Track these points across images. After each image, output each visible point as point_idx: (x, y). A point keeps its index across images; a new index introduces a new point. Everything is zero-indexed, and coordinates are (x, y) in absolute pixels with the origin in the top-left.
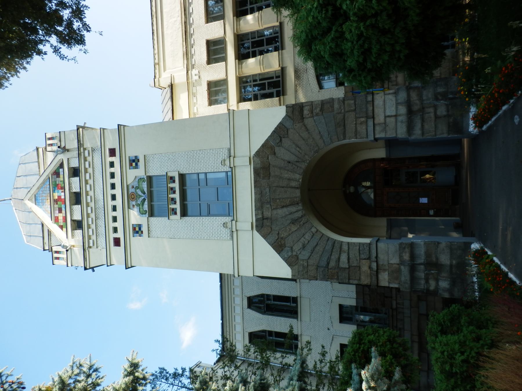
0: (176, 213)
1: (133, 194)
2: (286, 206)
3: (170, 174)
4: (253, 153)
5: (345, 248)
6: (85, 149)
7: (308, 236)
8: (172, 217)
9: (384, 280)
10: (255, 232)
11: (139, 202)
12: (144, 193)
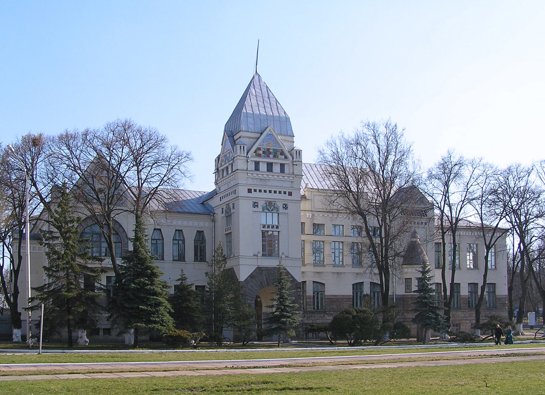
1: (272, 203)
3: (279, 227)
7: (256, 288)
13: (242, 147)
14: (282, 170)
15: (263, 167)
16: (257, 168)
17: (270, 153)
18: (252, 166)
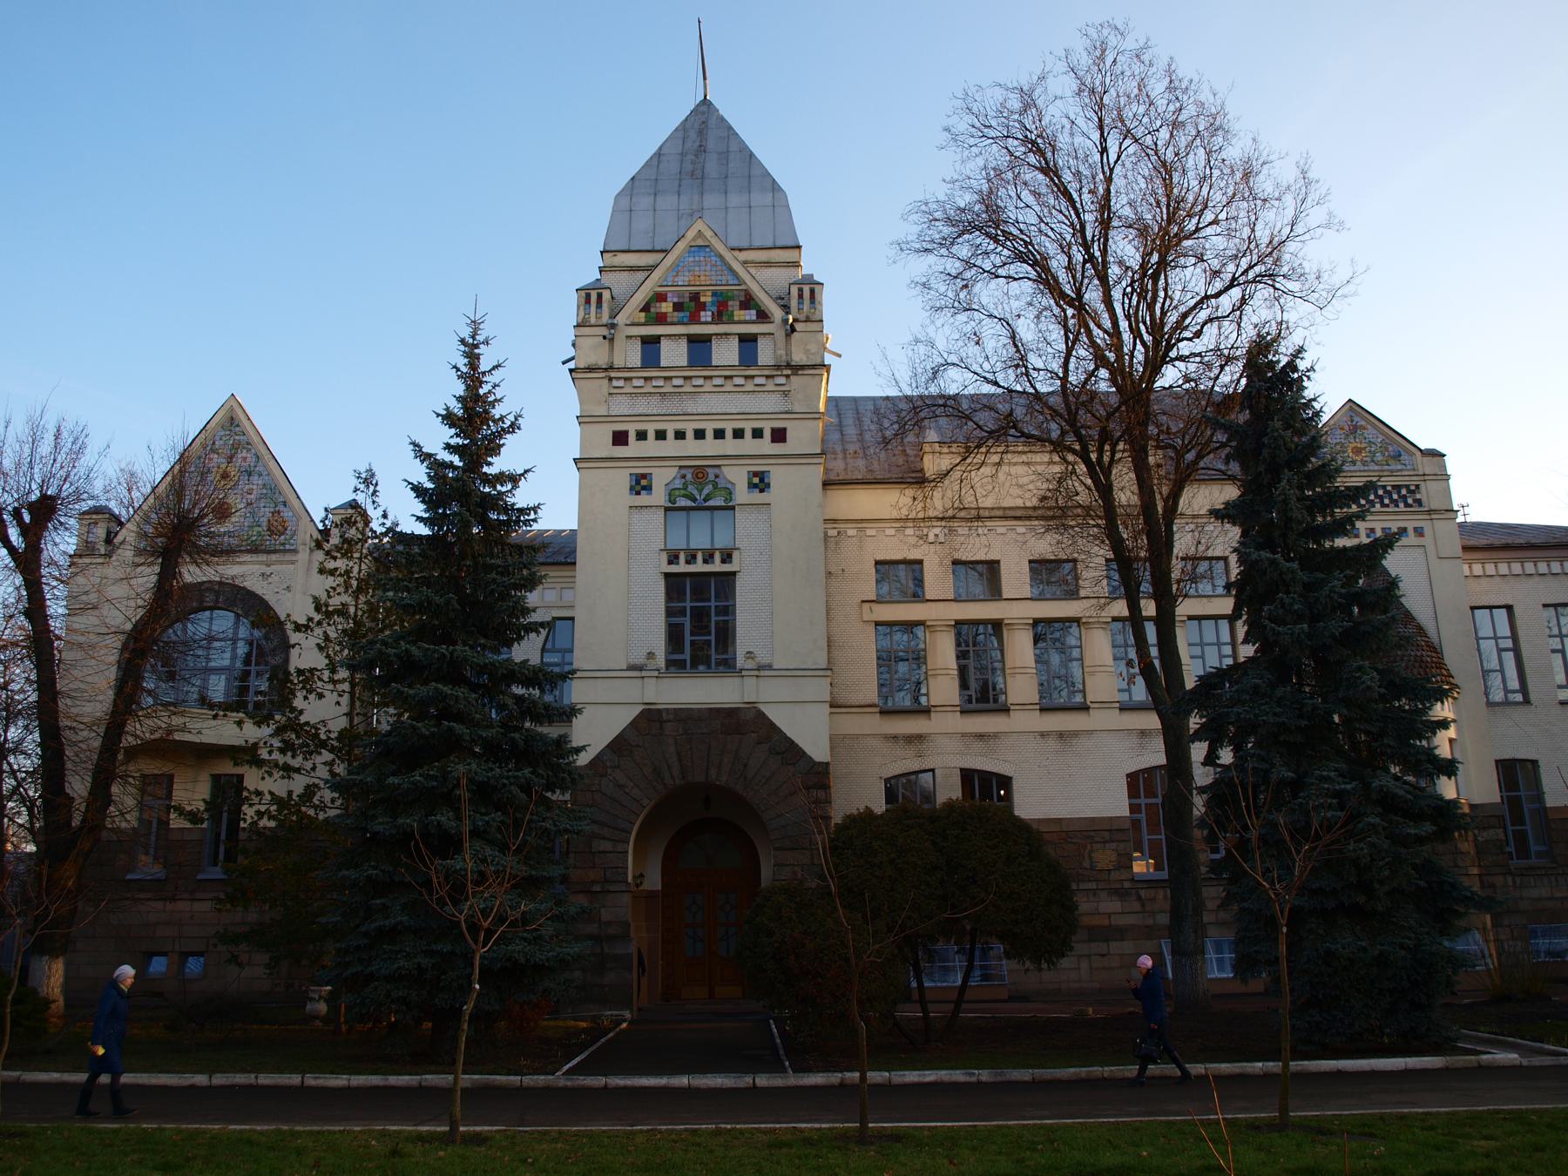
0: (670, 562)
1: (705, 475)
2: (680, 761)
3: (736, 555)
4: (763, 708)
5: (620, 848)
6: (788, 376)
8: (664, 557)
10: (641, 708)
11: (692, 489)
12: (705, 500)
13: (594, 298)
15: (674, 353)
17: (703, 306)
18: (634, 355)
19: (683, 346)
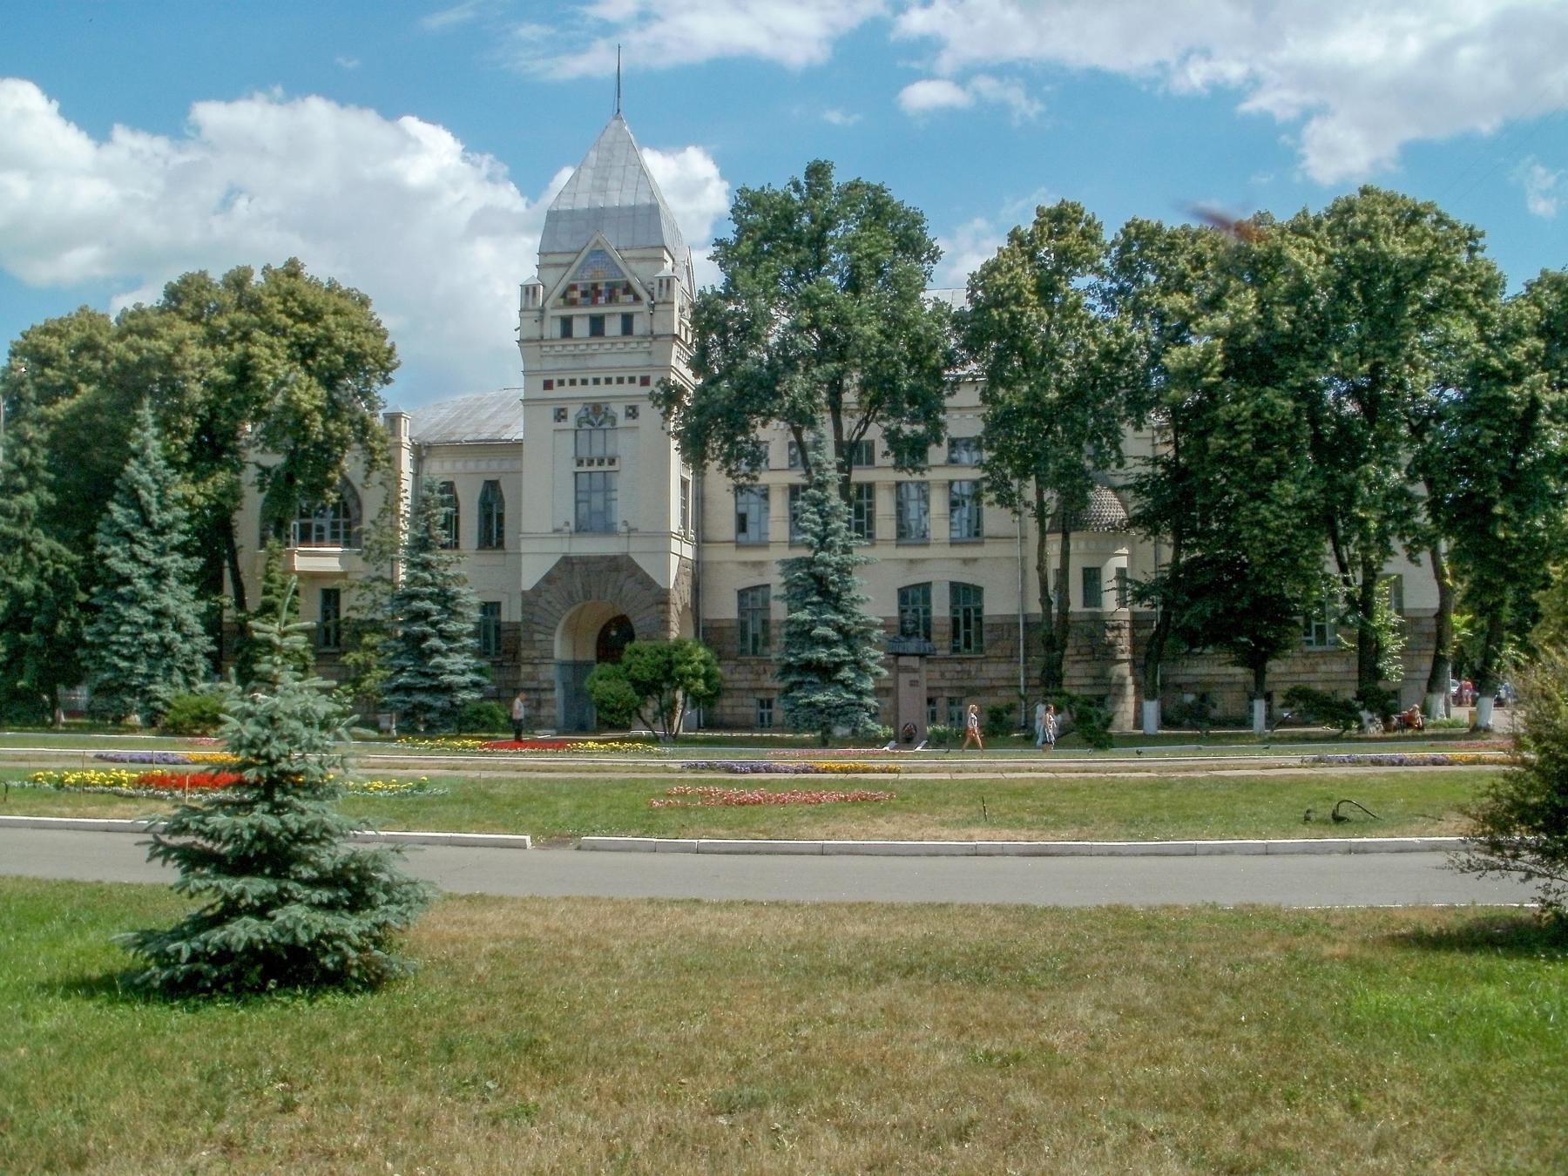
9: (526, 669)
14: (627, 327)
15: (581, 328)
16: (567, 330)
17: (599, 293)
18: (554, 329)
19: (587, 322)
